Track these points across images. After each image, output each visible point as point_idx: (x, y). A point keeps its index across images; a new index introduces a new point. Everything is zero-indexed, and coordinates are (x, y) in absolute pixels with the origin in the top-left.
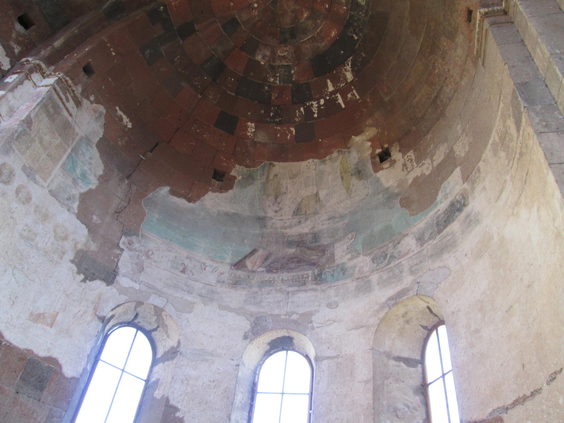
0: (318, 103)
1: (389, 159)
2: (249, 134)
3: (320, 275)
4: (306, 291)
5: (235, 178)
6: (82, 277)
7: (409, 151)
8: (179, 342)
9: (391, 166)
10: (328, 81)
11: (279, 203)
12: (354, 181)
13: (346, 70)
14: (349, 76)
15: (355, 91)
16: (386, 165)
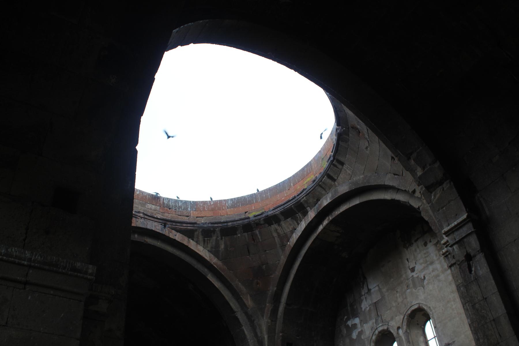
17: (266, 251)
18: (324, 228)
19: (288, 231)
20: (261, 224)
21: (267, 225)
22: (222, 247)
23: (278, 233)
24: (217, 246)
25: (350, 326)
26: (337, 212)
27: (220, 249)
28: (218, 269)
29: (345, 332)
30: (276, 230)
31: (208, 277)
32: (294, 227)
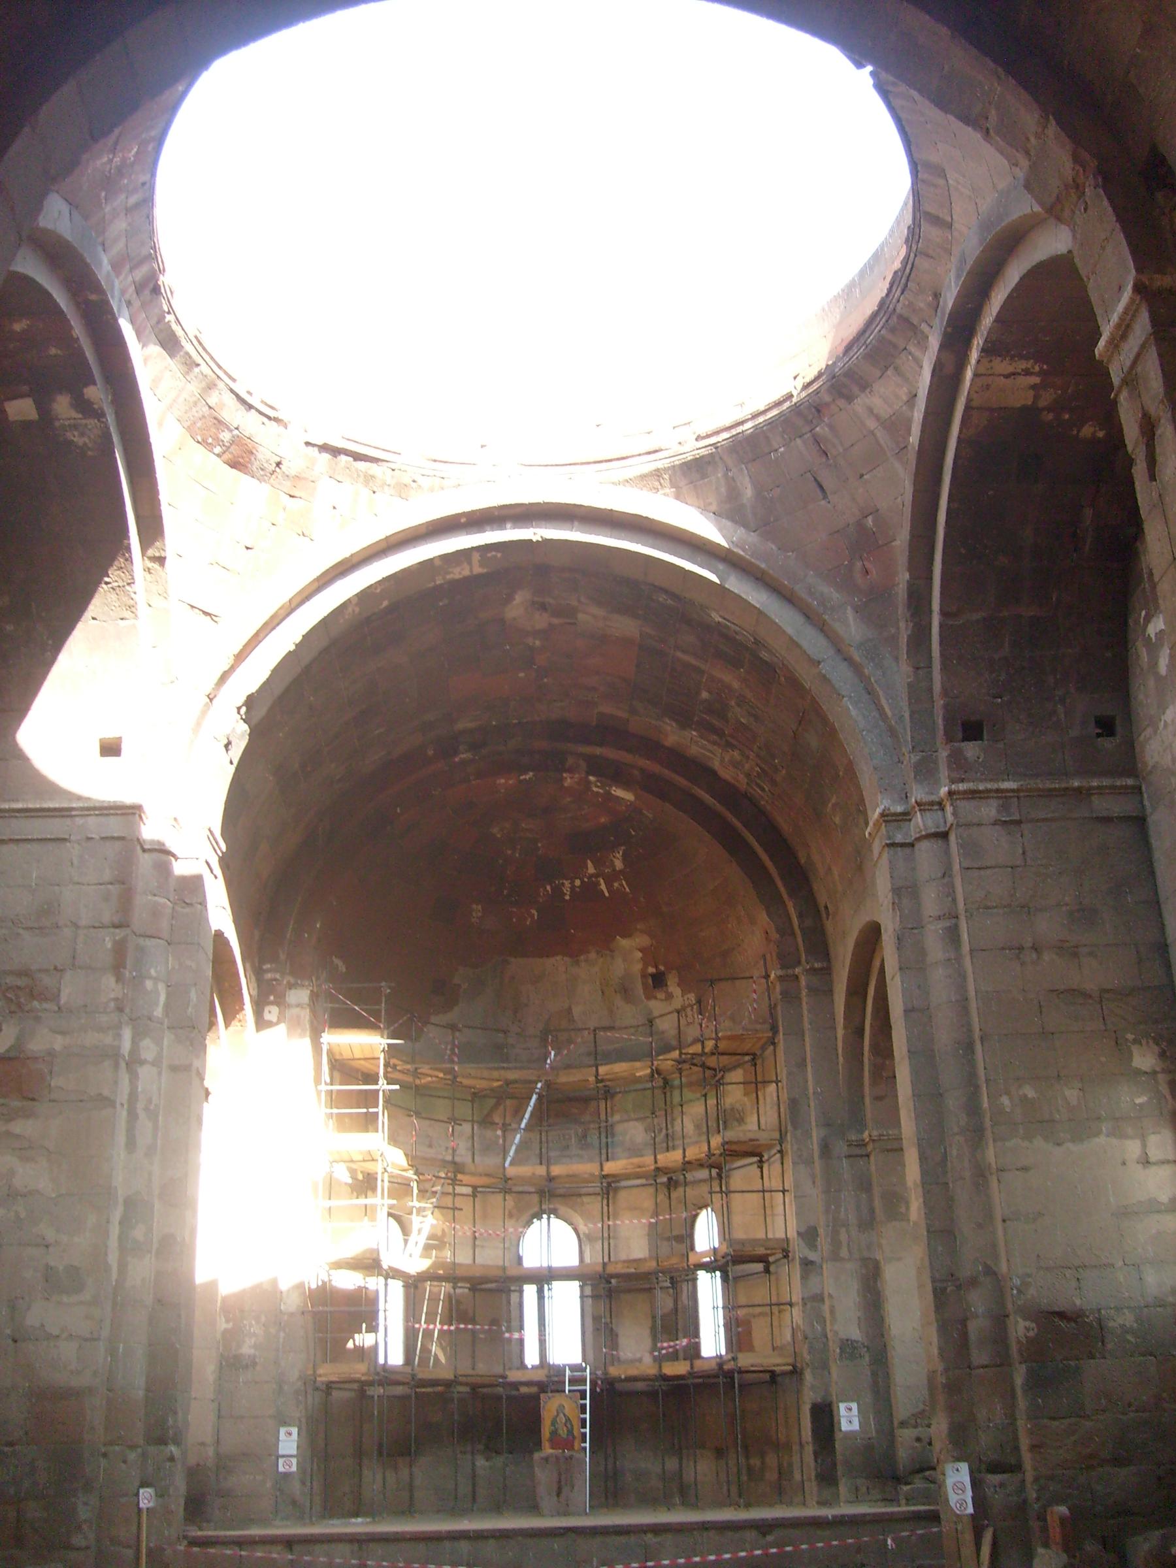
0: (572, 883)
1: (664, 988)
2: (473, 920)
3: (585, 1136)
4: (568, 1156)
5: (459, 986)
6: (355, 1194)
7: (690, 992)
8: (443, 1230)
9: (666, 999)
10: (589, 861)
11: (520, 1021)
12: (618, 1001)
13: (614, 857)
14: (619, 865)
15: (624, 882)
16: (661, 995)
17: (862, 476)
18: (976, 375)
19: (900, 404)
20: (827, 405)
21: (842, 403)
22: (748, 492)
23: (877, 418)
24: (733, 494)
25: (1154, 640)
26: (987, 320)
27: (745, 501)
28: (747, 557)
29: (1146, 660)
30: (870, 410)
31: (726, 586)
32: (910, 393)
